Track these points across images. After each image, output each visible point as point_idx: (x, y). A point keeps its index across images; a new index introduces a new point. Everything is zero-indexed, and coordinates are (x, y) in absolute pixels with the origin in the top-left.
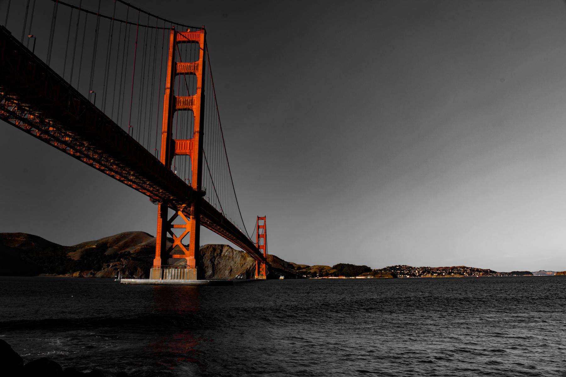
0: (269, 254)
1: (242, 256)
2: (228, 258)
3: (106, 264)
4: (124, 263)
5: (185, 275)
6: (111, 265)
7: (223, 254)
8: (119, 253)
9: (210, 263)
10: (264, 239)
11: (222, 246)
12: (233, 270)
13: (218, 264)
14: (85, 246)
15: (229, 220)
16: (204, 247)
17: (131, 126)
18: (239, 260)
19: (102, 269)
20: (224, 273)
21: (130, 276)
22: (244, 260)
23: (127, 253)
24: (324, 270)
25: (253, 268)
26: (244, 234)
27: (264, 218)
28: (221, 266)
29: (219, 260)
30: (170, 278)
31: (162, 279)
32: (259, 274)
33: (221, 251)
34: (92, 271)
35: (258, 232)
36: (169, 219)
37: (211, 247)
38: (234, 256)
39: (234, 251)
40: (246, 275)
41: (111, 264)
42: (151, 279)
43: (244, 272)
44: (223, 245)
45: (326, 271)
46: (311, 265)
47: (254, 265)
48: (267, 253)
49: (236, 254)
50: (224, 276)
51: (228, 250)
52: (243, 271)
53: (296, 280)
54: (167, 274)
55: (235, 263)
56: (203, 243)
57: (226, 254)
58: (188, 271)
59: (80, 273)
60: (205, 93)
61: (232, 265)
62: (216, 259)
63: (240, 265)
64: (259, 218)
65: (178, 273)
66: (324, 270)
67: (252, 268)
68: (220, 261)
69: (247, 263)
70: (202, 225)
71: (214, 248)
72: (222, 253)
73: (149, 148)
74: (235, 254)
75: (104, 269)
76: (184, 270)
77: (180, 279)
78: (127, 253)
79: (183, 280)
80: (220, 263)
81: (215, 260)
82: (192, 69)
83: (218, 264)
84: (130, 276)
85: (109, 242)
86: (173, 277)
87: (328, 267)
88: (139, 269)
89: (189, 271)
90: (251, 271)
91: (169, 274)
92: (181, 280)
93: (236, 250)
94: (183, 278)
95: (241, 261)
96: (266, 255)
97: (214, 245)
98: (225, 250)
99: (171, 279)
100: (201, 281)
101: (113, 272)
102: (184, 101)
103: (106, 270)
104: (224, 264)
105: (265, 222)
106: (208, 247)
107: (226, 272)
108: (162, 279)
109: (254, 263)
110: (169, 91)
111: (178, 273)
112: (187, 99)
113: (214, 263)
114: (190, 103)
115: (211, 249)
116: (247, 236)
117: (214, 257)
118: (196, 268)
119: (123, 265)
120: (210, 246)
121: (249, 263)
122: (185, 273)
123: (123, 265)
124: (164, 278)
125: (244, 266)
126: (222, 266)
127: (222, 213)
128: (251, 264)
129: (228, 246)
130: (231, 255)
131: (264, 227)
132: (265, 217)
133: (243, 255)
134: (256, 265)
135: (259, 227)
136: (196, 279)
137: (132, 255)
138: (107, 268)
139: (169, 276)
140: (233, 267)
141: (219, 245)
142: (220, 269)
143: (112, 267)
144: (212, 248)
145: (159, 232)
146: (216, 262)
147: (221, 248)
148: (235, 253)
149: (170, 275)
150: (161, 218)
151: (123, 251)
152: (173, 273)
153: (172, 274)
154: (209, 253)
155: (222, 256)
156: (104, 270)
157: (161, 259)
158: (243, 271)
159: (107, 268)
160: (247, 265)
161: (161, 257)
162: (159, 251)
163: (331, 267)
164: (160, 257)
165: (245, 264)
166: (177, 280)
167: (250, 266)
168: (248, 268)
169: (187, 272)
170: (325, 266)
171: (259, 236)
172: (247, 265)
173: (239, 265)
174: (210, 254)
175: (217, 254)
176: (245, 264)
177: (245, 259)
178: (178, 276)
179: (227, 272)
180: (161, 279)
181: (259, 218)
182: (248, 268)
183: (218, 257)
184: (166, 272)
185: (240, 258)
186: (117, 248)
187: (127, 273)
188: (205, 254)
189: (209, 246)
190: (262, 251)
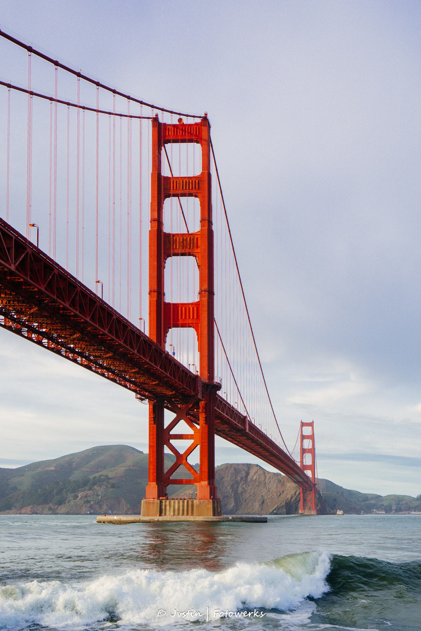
0: (320, 477)
1: (280, 481)
2: (257, 483)
3: (72, 495)
4: (100, 493)
5: (195, 509)
6: (80, 495)
7: (250, 477)
8: (91, 477)
9: (231, 491)
10: (312, 455)
11: (249, 466)
12: (265, 502)
13: (242, 493)
14: (37, 468)
15: (259, 427)
16: (221, 468)
17: (98, 282)
18: (274, 487)
19: (67, 501)
20: (252, 505)
21: (110, 512)
22: (282, 486)
23: (103, 477)
24: (403, 502)
25: (296, 499)
26: (282, 448)
27: (311, 424)
28: (247, 496)
29: (244, 486)
30: (172, 514)
31: (160, 515)
32: (306, 508)
33: (247, 474)
34: (51, 505)
36: (167, 426)
37: (231, 467)
38: (266, 480)
39: (266, 474)
40: (286, 509)
41: (79, 495)
42: (144, 516)
43: (282, 504)
44: (250, 464)
45: (407, 503)
46: (383, 494)
47: (297, 493)
48: (316, 477)
49: (270, 477)
50: (253, 510)
51: (257, 472)
52: (281, 503)
53: (360, 515)
54: (168, 508)
55: (269, 491)
56: (219, 462)
57: (255, 477)
58: (198, 504)
59: (31, 508)
60: (214, 228)
61: (263, 494)
62: (240, 485)
63: (277, 494)
64: (303, 424)
65: (183, 506)
66: (403, 502)
67: (294, 499)
68: (246, 489)
69: (286, 491)
70: (218, 435)
71: (235, 469)
72: (249, 477)
73: (129, 318)
74: (267, 478)
75: (69, 501)
76: (193, 502)
77: (187, 514)
78: (103, 477)
79: (191, 517)
80: (245, 491)
81: (238, 488)
82: (191, 188)
83: (242, 493)
84: (110, 512)
85: (74, 462)
86: (176, 513)
87: (410, 497)
88: (123, 501)
89: (200, 503)
90: (293, 503)
91: (170, 508)
92: (188, 517)
93: (269, 473)
94: (192, 514)
95: (278, 488)
96: (316, 479)
97: (236, 464)
98: (252, 473)
99: (174, 515)
100: (219, 518)
101: (83, 505)
102: (181, 240)
103: (72, 503)
104: (252, 493)
105: (313, 429)
106: (227, 467)
107: (254, 504)
108: (160, 515)
109: (297, 491)
110: (157, 224)
111: (183, 506)
112: (185, 238)
113: (237, 490)
114: (190, 244)
115: (232, 470)
116: (285, 451)
117: (237, 483)
118: (210, 499)
119: (98, 495)
120: (229, 467)
121: (290, 490)
122: (195, 506)
123: (98, 495)
124: (163, 514)
125: (282, 496)
126: (249, 495)
127: (248, 416)
128: (293, 492)
129: (257, 465)
130: (263, 479)
131: (312, 437)
133: (280, 479)
134: (299, 494)
135: (303, 437)
136: (211, 512)
137: (111, 481)
138: (73, 499)
139: (170, 510)
140: (266, 497)
141: (243, 464)
142: (245, 500)
143: (81, 499)
144: (232, 469)
145: (153, 446)
146: (240, 490)
147: (246, 469)
148: (268, 476)
149: (172, 509)
150: (154, 424)
151: (97, 475)
152: (176, 507)
153: (174, 508)
154: (229, 477)
155: (248, 480)
156: (68, 504)
157: (157, 486)
158: (281, 503)
159: (73, 499)
160: (287, 493)
161: (157, 484)
162: (153, 474)
163: (413, 498)
164: (155, 483)
165: (283, 492)
166: (182, 517)
167: (292, 496)
168: (288, 498)
169: (197, 505)
170: (405, 496)
171: (303, 451)
172: (287, 493)
173: (275, 494)
174: (231, 477)
175: (242, 479)
176: (284, 493)
177: (283, 485)
178: (183, 510)
179: (257, 505)
180: (158, 515)
181: (303, 424)
182: (288, 498)
183: (243, 483)
184: (166, 506)
185: (276, 483)
186: (88, 470)
187: (105, 507)
188: (223, 478)
189: (228, 466)
190: (309, 473)
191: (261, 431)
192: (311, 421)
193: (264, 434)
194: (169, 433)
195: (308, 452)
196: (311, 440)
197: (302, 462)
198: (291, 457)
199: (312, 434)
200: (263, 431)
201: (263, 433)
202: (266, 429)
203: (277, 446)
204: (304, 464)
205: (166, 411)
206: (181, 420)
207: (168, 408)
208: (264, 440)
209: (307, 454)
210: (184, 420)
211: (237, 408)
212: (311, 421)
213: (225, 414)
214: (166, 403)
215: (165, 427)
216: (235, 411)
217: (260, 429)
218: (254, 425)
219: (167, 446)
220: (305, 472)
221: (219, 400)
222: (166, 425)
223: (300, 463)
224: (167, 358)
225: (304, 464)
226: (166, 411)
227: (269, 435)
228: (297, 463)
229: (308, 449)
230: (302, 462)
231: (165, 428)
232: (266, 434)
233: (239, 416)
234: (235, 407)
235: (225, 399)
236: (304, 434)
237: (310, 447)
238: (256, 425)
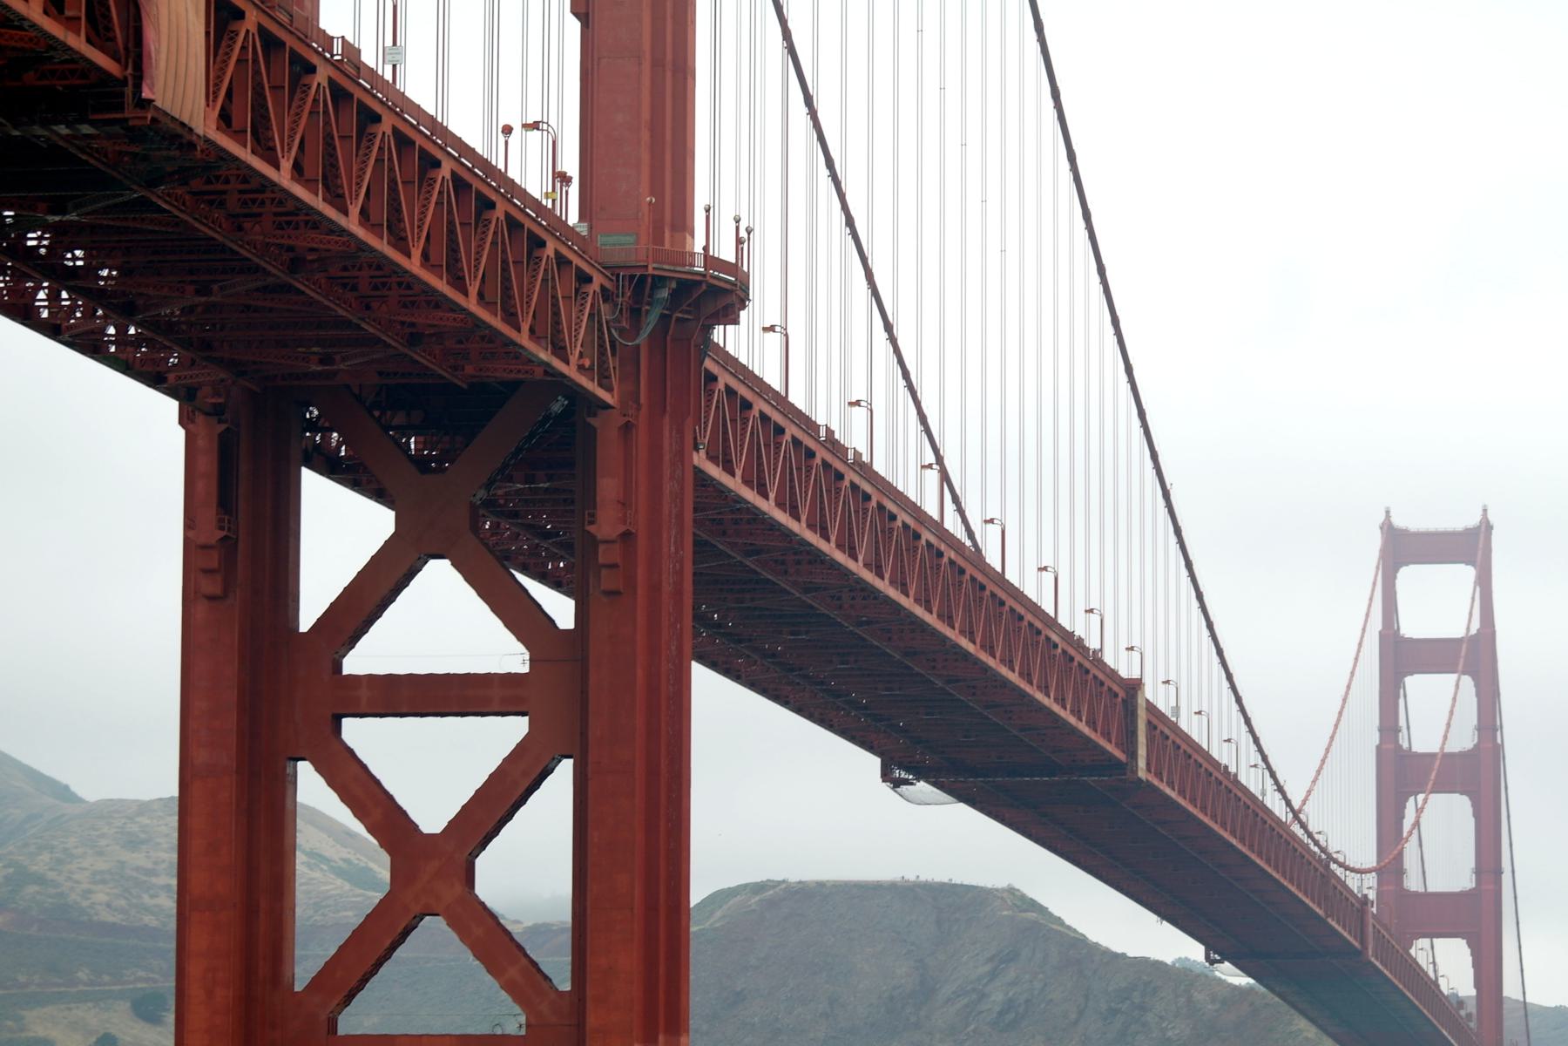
35: (1390, 724)
48: (1510, 989)
116: (1253, 779)
132: (1486, 527)
191: (1052, 623)
192: (1472, 520)
193: (1079, 644)
194: (338, 667)
195: (1444, 786)
196: (1467, 681)
197: (1390, 867)
198: (1299, 832)
199: (1475, 626)
200: (1071, 619)
201: (1068, 636)
202: (1172, 677)
203: (1187, 738)
204: (1413, 883)
205: (316, 490)
206: (432, 563)
207: (333, 468)
208: (1077, 700)
209: (1437, 800)
210: (457, 565)
211: (863, 448)
212: (1462, 519)
213: (768, 506)
214: (313, 426)
215: (306, 622)
216: (851, 476)
217: (1049, 608)
218: (1000, 579)
219: (319, 769)
220: (1420, 950)
221: (730, 392)
222: (312, 604)
223: (1371, 880)
224: (349, 96)
225: (1413, 883)
226: (316, 490)
227: (1124, 654)
228: (1353, 882)
229: (1448, 757)
230: (1390, 867)
231: (306, 622)
232: (1093, 643)
233: (881, 507)
234: (855, 439)
235: (773, 380)
236: (1413, 626)
237: (1464, 739)
238: (1012, 576)
